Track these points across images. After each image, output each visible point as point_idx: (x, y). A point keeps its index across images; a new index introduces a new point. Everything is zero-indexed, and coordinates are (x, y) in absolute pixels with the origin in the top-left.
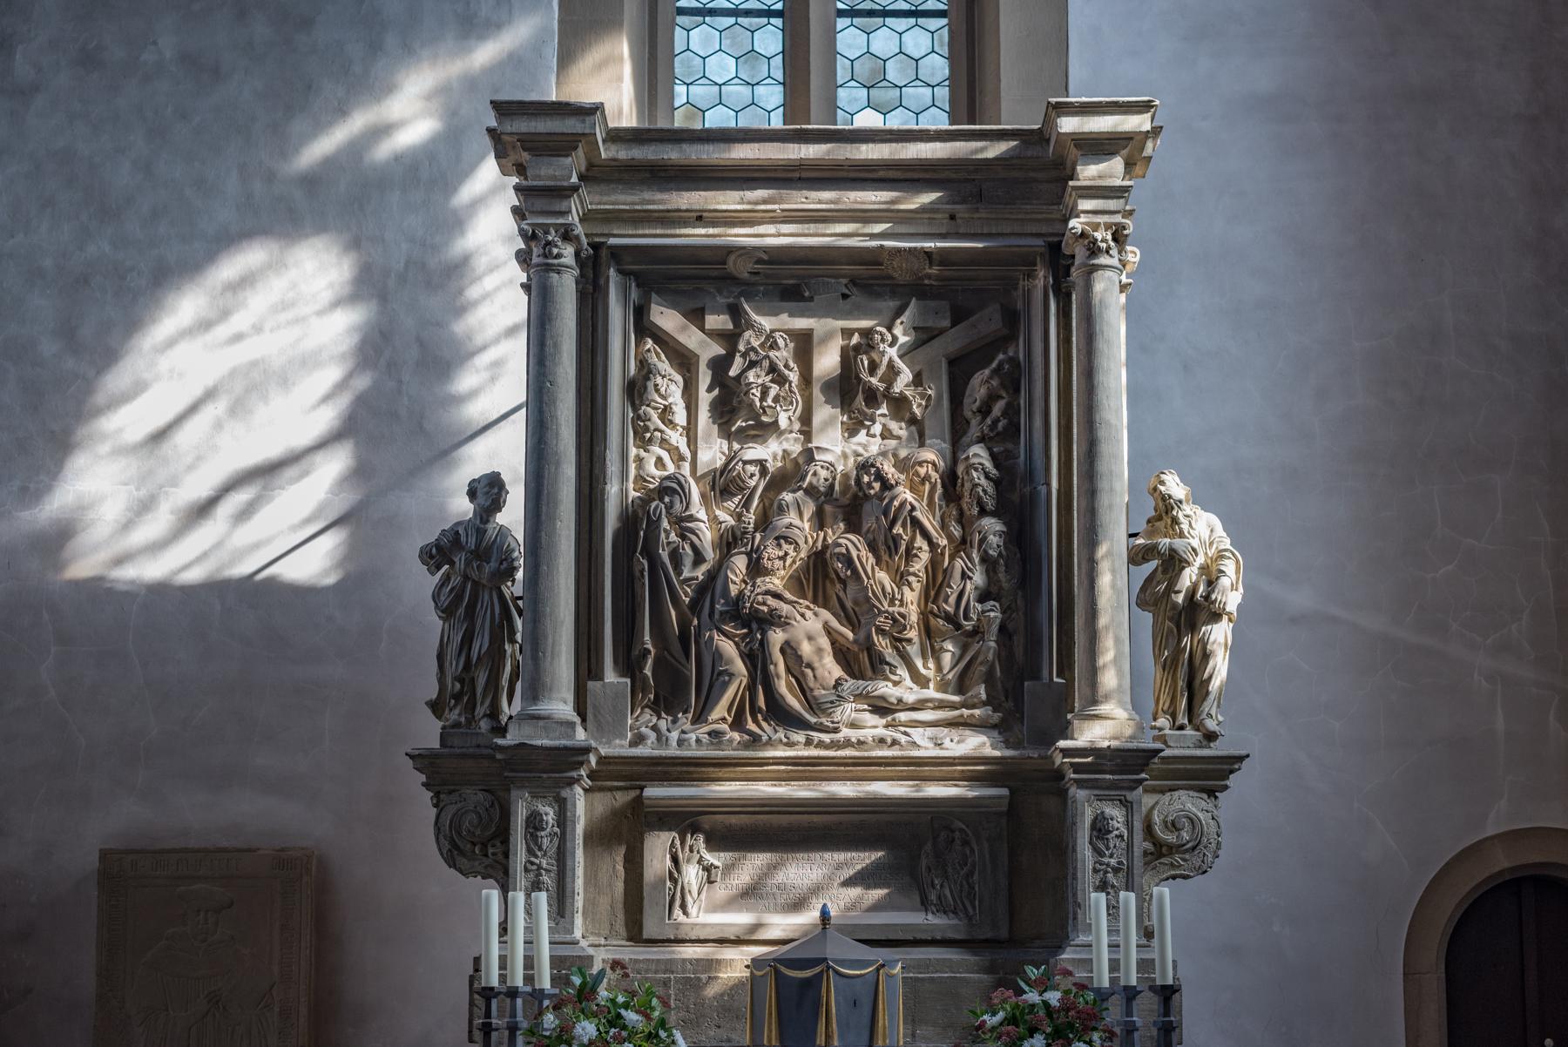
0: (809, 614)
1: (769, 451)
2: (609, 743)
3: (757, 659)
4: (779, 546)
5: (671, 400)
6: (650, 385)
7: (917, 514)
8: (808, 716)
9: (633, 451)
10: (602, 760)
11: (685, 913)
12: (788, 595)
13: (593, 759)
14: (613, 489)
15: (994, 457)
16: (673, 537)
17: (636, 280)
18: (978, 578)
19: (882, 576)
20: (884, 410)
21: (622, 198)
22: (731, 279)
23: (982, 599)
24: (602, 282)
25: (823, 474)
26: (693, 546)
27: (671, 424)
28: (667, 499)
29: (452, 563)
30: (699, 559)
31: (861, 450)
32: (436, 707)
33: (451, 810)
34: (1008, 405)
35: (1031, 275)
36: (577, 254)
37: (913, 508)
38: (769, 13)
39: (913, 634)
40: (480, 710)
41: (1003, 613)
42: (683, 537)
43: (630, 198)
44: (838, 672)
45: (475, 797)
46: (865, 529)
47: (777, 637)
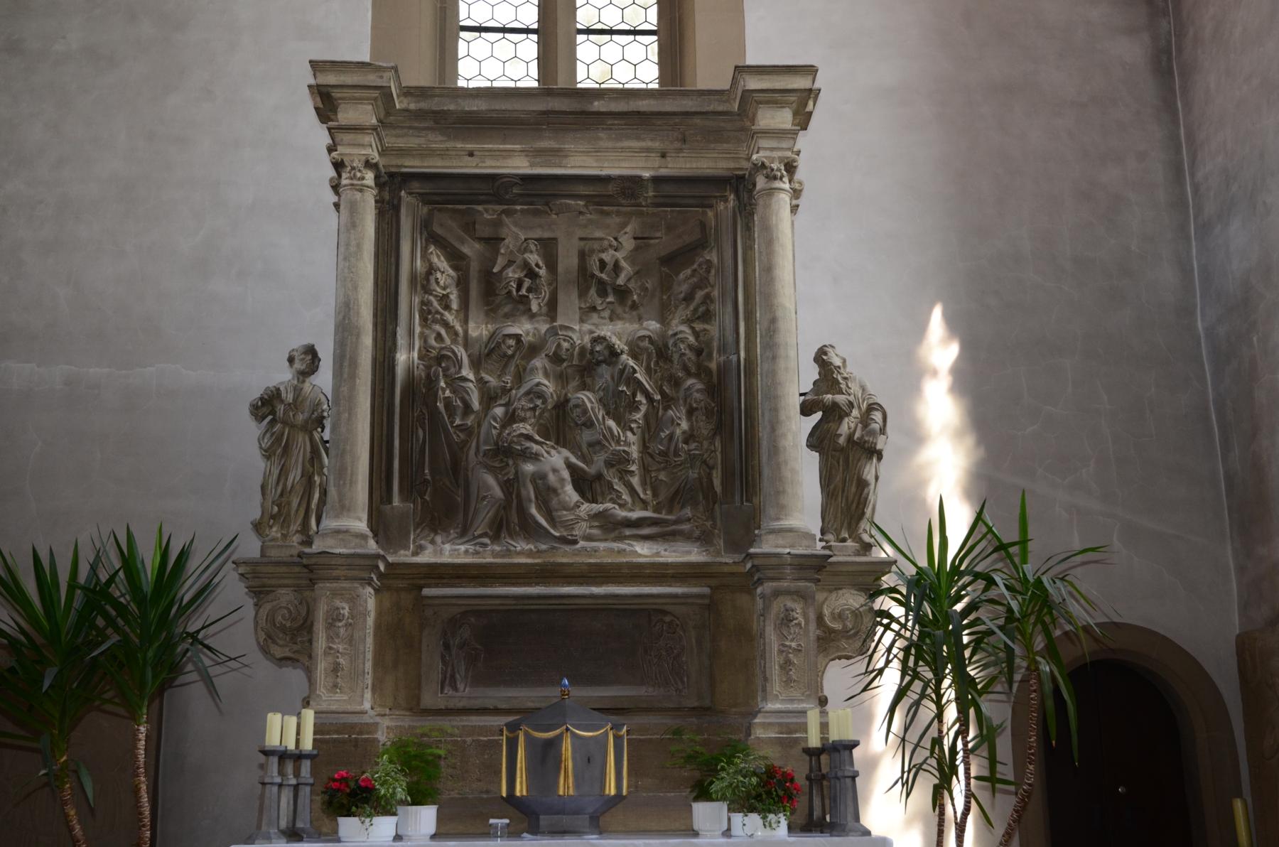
0: (553, 452)
1: (523, 328)
2: (395, 552)
3: (511, 486)
4: (531, 401)
7: (637, 375)
8: (552, 531)
9: (418, 330)
10: (388, 565)
11: (456, 689)
12: (537, 438)
13: (382, 568)
14: (402, 358)
15: (696, 334)
16: (448, 393)
18: (685, 425)
19: (611, 423)
20: (610, 299)
23: (686, 442)
25: (565, 345)
27: (447, 307)
29: (273, 412)
30: (467, 408)
31: (593, 328)
32: (258, 527)
33: (268, 607)
36: (377, 178)
37: (635, 371)
38: (527, 31)
45: (286, 597)
47: (529, 468)
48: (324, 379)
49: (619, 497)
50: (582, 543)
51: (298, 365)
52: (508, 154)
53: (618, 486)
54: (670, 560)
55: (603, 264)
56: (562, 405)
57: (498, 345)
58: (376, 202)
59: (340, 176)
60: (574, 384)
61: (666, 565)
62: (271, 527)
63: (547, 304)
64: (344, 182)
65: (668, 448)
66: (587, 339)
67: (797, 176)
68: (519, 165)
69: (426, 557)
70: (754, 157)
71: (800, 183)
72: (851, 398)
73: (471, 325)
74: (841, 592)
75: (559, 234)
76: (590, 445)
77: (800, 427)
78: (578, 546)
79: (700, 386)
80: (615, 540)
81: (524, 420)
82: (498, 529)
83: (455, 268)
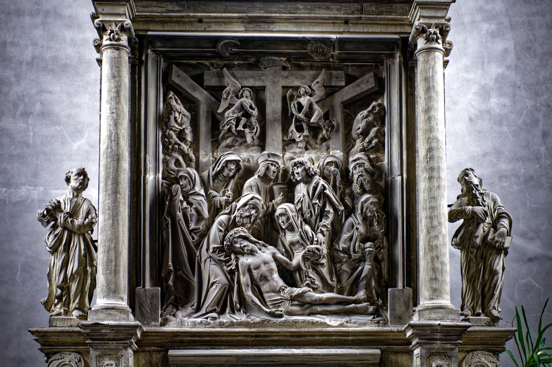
0: (263, 249)
1: (242, 155)
2: (148, 324)
5: (184, 126)
6: (172, 117)
7: (327, 191)
9: (161, 156)
10: (144, 333)
12: (253, 239)
14: (150, 177)
15: (370, 160)
16: (185, 204)
17: (164, 57)
18: (362, 229)
19: (307, 228)
20: (306, 133)
21: (155, 9)
24: (144, 58)
25: (273, 168)
26: (197, 210)
28: (181, 183)
29: (56, 220)
33: (56, 363)
34: (378, 131)
35: (392, 56)
36: (129, 40)
37: (325, 188)
39: (324, 261)
40: (73, 306)
41: (377, 249)
42: (190, 204)
43: (160, 10)
46: (296, 201)
48: (92, 193)
49: (313, 283)
50: (286, 318)
51: (74, 183)
52: (228, 21)
54: (351, 329)
55: (300, 107)
56: (270, 215)
57: (223, 169)
58: (129, 58)
59: (101, 38)
61: (347, 334)
62: (56, 305)
63: (259, 138)
64: (105, 42)
65: (349, 247)
66: (289, 164)
67: (448, 39)
68: (239, 32)
69: (172, 327)
70: (417, 23)
71: (450, 44)
72: (486, 209)
73: (202, 153)
74: (476, 353)
75: (268, 84)
76: (292, 244)
77: (447, 229)
78: (283, 319)
80: (309, 315)
81: (243, 225)
82: (222, 305)
83: (188, 111)
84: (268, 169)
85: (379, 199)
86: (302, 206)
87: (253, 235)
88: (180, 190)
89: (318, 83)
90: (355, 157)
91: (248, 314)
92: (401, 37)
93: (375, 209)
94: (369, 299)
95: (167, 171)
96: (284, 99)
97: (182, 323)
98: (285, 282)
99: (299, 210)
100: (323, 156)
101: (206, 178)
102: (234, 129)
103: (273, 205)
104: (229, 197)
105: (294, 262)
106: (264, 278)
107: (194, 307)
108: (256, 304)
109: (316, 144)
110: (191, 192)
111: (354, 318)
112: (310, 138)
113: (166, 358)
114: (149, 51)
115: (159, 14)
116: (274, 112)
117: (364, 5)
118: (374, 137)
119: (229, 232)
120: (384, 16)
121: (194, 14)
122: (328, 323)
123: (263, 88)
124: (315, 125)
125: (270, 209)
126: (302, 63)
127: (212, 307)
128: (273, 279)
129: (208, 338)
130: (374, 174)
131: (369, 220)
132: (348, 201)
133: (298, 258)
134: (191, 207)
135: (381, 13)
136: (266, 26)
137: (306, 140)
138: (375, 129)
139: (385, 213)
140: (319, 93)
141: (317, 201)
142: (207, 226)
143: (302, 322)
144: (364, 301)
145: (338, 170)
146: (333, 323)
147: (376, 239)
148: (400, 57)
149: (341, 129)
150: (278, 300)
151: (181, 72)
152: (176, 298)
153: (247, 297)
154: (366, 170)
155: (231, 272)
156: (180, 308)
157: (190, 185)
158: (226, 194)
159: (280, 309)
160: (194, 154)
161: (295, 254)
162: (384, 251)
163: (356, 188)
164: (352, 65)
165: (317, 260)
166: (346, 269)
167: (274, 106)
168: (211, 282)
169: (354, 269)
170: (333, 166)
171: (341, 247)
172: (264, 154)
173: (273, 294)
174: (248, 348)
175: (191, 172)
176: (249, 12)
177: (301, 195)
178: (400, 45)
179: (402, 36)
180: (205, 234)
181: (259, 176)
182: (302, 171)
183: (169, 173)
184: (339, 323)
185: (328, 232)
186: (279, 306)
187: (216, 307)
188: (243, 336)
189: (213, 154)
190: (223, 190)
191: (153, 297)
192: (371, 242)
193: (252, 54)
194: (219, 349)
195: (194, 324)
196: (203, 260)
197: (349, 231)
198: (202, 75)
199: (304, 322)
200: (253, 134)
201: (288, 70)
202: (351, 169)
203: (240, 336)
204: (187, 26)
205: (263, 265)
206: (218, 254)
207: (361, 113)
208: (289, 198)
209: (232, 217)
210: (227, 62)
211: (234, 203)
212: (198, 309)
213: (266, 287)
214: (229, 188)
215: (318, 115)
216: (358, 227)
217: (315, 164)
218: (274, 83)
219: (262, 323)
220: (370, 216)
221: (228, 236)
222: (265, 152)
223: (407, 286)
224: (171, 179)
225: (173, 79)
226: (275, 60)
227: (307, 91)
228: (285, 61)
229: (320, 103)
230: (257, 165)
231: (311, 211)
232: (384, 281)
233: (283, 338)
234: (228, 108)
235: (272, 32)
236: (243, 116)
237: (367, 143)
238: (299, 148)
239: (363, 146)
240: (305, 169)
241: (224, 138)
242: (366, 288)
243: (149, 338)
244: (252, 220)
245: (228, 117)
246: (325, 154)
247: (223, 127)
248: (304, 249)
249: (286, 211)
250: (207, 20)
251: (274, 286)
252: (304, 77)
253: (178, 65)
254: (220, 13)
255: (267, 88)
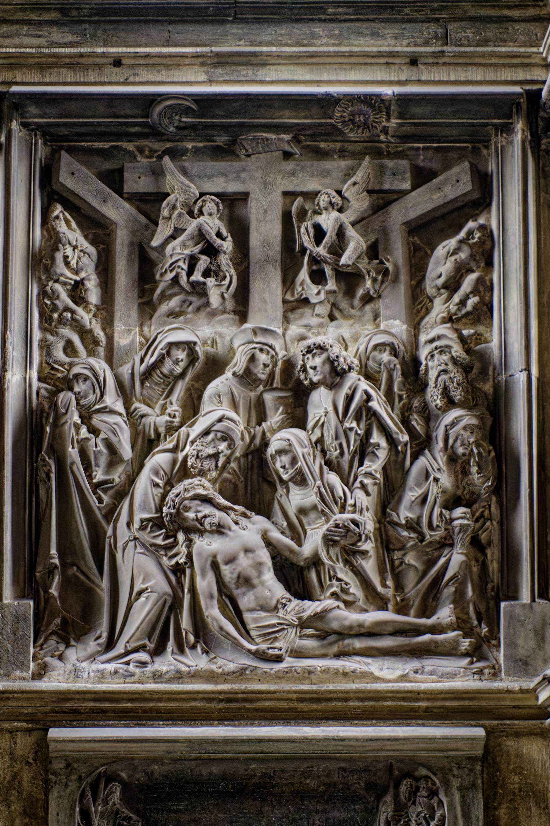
0: (243, 521)
5: (83, 275)
6: (59, 256)
7: (374, 404)
9: (37, 335)
15: (462, 340)
16: (84, 432)
17: (43, 135)
18: (446, 480)
19: (333, 478)
21: (27, 40)
22: (155, 133)
25: (263, 358)
28: (76, 389)
34: (479, 281)
35: (507, 129)
39: (368, 546)
41: (477, 521)
42: (95, 431)
43: (36, 41)
44: (279, 591)
46: (310, 425)
47: (205, 546)
49: (345, 591)
50: (289, 662)
52: (174, 62)
53: (343, 573)
54: (423, 686)
55: (319, 234)
57: (161, 360)
60: (275, 418)
61: (416, 695)
63: (235, 296)
65: (420, 517)
68: (194, 82)
69: (56, 681)
73: (119, 327)
75: (254, 189)
76: (302, 511)
78: (282, 666)
79: (469, 420)
80: (337, 656)
81: (202, 473)
82: (160, 636)
83: (93, 243)
84: (253, 359)
85: (481, 418)
86: (322, 434)
87: (221, 492)
88: (74, 403)
89: (355, 184)
90: (432, 334)
91: (212, 655)
92: (526, 91)
93: (472, 440)
94: (461, 624)
95: (48, 364)
96: (287, 217)
97: (76, 674)
98: (288, 588)
99: (316, 443)
100: (367, 332)
101: (126, 378)
102: (185, 278)
103: (264, 433)
104: (174, 417)
105: (307, 550)
106: (245, 581)
107: (101, 641)
108: (228, 635)
109: (353, 307)
110: (97, 407)
111: (430, 663)
112: (340, 296)
113: (42, 746)
114: (14, 125)
115: (33, 51)
116: (266, 244)
117: (450, 27)
118: (471, 292)
119: (172, 487)
120: (490, 49)
121: (105, 50)
122: (377, 673)
123: (244, 197)
124: (349, 270)
125: (258, 441)
126: (323, 145)
127: (139, 639)
128: (262, 583)
129: (129, 705)
130: (471, 369)
131: (460, 461)
132: (417, 423)
133: (313, 542)
134: (97, 436)
135: (485, 42)
136: (250, 72)
137: (332, 299)
138: (471, 278)
139: (495, 448)
140: (359, 203)
141: (354, 425)
142: (128, 476)
143: (323, 672)
144: (451, 627)
145: (396, 361)
146: (388, 674)
147: (475, 501)
148: (523, 131)
149: (404, 277)
150: (273, 626)
151: (76, 166)
152: (65, 622)
153: (209, 620)
154: (454, 361)
155: (178, 570)
156: (73, 643)
157: (94, 392)
158: (168, 411)
159: (277, 644)
160: (104, 330)
161: (309, 532)
162: (493, 526)
163: (434, 396)
164: (425, 149)
165: (354, 544)
166: (413, 562)
167: (265, 232)
168: (136, 590)
169: (431, 563)
170: (387, 352)
171: (402, 517)
172: (244, 331)
173: (263, 614)
174: (212, 725)
175: (97, 366)
176: (215, 44)
177: (322, 412)
178: (524, 106)
179: (528, 87)
180: (124, 491)
181: (234, 374)
182: (324, 363)
183: (53, 368)
184: (399, 673)
185: (376, 488)
186: (276, 638)
187: (146, 641)
188: (202, 699)
189: (141, 330)
190: (161, 402)
191: (17, 619)
192: (465, 506)
193: (221, 127)
194: (152, 726)
195: (102, 676)
196: (120, 544)
197: (418, 485)
198: (121, 171)
199: (326, 671)
200: (223, 289)
201: (295, 159)
202: (422, 358)
203: (195, 700)
204: (91, 73)
205: (242, 555)
206: (151, 531)
207: (443, 244)
208: (297, 419)
209: (180, 456)
210: (169, 145)
211: (184, 429)
212: (110, 644)
213: (249, 601)
214: (174, 398)
215: (355, 249)
216: (438, 475)
217: (350, 349)
218: (266, 184)
219: (241, 674)
220: (464, 454)
221: (171, 495)
222: (246, 326)
223: (541, 596)
224: (57, 381)
225: (61, 179)
226: (267, 139)
227: (333, 200)
228: (288, 142)
229: (358, 226)
230: (232, 351)
231: (341, 445)
232: (493, 589)
233: (283, 704)
234: (173, 237)
235: (263, 82)
236: (202, 252)
237: (457, 304)
238: (318, 315)
239: (449, 312)
240: (328, 358)
241: (163, 297)
242: (454, 602)
243: (10, 703)
244: (220, 463)
245: (171, 256)
246: (370, 327)
247: (162, 275)
248: (327, 521)
249: (290, 445)
250: (132, 62)
251: (265, 598)
252: (326, 174)
253: (70, 151)
254: (157, 45)
255: (251, 195)
